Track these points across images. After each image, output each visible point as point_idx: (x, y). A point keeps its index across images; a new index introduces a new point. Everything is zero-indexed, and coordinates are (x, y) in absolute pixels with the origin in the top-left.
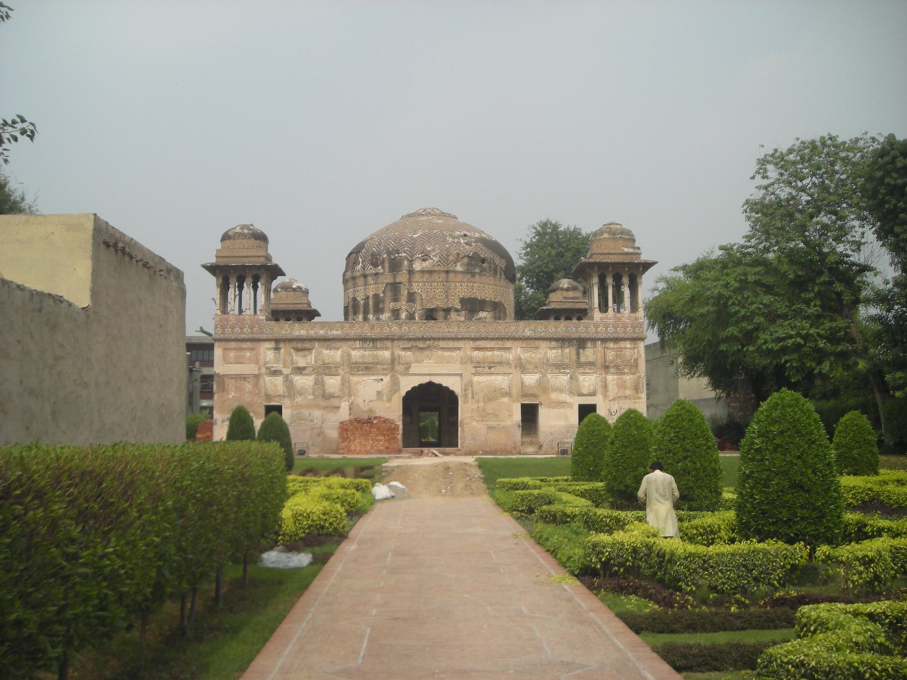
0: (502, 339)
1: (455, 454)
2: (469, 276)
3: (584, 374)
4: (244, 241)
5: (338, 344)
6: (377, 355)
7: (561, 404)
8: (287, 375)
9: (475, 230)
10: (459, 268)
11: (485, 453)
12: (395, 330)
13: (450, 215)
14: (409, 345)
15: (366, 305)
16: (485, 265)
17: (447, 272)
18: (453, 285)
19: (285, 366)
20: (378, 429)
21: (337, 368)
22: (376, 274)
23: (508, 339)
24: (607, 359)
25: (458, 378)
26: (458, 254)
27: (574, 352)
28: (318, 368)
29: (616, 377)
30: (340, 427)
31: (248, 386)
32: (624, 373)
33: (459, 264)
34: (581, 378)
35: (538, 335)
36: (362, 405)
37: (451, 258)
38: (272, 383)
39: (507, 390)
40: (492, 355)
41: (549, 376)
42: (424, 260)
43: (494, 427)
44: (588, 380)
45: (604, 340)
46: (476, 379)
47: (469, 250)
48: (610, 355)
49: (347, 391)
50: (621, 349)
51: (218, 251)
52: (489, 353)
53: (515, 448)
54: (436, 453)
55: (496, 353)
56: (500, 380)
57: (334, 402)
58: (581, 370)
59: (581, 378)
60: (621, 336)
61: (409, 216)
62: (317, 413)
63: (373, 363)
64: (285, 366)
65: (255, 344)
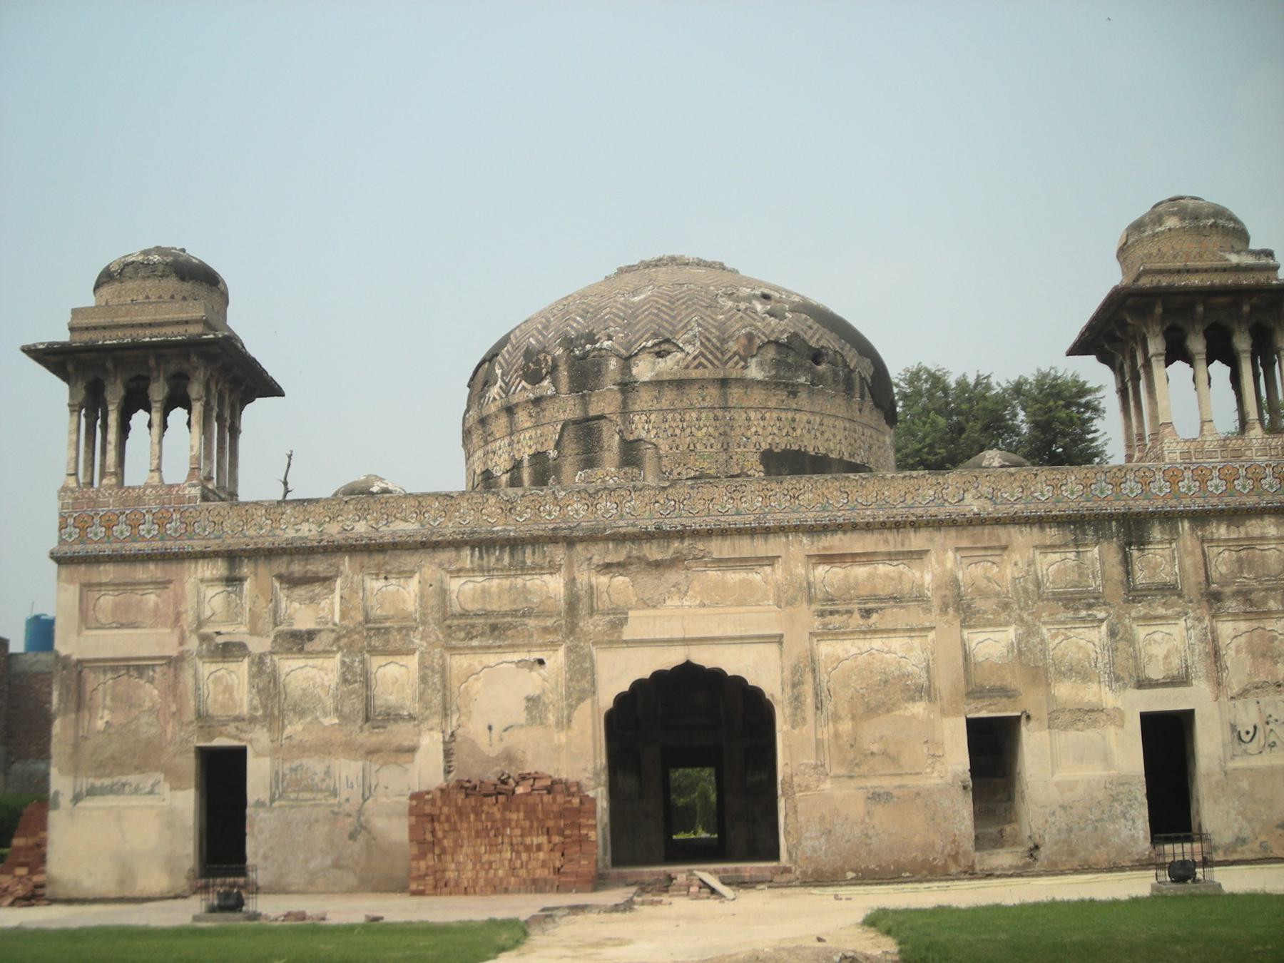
0: (898, 526)
1: (770, 883)
2: (783, 395)
3: (1148, 619)
4: (149, 283)
5: (409, 560)
6: (525, 590)
7: (1089, 714)
8: (261, 657)
9: (789, 293)
10: (755, 371)
11: (869, 877)
12: (578, 513)
13: (722, 267)
14: (617, 554)
15: (515, 482)
16: (822, 368)
17: (724, 383)
18: (740, 417)
19: (253, 632)
20: (530, 812)
21: (405, 630)
22: (537, 401)
23: (915, 525)
24: (1214, 575)
25: (771, 650)
26: (750, 337)
27: (1114, 557)
28: (350, 632)
29: (1243, 626)
30: (412, 811)
31: (150, 693)
32: (1268, 614)
33: (753, 362)
34: (1141, 632)
35: (1003, 510)
36: (482, 740)
37: (733, 346)
38: (217, 681)
39: (923, 681)
40: (871, 577)
41: (1044, 630)
42: (660, 355)
43: (887, 794)
44: (1166, 640)
45: (1200, 518)
46: (826, 649)
47: (781, 328)
48: (1222, 562)
49: (436, 700)
50: (1250, 543)
51: (75, 312)
52: (861, 571)
53: (955, 858)
54: (714, 882)
55: (882, 569)
56: (899, 652)
57: (400, 734)
58: (1140, 609)
59: (1141, 632)
60: (1251, 501)
61: (622, 271)
62: (348, 769)
63: (514, 613)
64: (253, 632)
65: (173, 568)
